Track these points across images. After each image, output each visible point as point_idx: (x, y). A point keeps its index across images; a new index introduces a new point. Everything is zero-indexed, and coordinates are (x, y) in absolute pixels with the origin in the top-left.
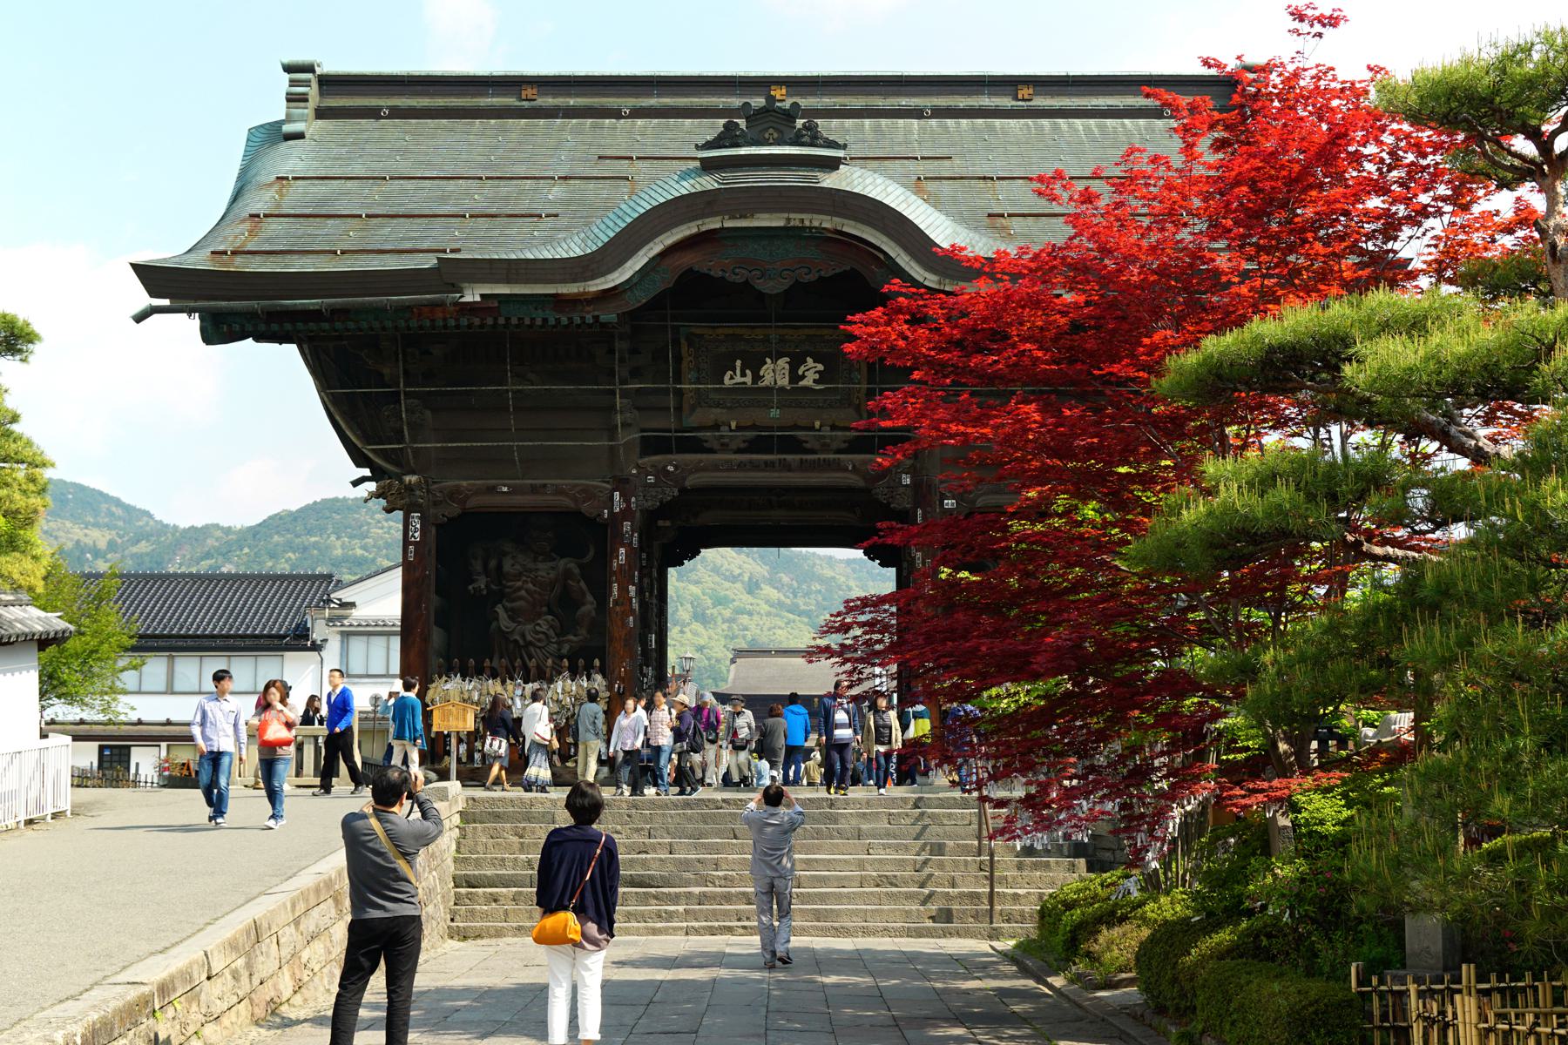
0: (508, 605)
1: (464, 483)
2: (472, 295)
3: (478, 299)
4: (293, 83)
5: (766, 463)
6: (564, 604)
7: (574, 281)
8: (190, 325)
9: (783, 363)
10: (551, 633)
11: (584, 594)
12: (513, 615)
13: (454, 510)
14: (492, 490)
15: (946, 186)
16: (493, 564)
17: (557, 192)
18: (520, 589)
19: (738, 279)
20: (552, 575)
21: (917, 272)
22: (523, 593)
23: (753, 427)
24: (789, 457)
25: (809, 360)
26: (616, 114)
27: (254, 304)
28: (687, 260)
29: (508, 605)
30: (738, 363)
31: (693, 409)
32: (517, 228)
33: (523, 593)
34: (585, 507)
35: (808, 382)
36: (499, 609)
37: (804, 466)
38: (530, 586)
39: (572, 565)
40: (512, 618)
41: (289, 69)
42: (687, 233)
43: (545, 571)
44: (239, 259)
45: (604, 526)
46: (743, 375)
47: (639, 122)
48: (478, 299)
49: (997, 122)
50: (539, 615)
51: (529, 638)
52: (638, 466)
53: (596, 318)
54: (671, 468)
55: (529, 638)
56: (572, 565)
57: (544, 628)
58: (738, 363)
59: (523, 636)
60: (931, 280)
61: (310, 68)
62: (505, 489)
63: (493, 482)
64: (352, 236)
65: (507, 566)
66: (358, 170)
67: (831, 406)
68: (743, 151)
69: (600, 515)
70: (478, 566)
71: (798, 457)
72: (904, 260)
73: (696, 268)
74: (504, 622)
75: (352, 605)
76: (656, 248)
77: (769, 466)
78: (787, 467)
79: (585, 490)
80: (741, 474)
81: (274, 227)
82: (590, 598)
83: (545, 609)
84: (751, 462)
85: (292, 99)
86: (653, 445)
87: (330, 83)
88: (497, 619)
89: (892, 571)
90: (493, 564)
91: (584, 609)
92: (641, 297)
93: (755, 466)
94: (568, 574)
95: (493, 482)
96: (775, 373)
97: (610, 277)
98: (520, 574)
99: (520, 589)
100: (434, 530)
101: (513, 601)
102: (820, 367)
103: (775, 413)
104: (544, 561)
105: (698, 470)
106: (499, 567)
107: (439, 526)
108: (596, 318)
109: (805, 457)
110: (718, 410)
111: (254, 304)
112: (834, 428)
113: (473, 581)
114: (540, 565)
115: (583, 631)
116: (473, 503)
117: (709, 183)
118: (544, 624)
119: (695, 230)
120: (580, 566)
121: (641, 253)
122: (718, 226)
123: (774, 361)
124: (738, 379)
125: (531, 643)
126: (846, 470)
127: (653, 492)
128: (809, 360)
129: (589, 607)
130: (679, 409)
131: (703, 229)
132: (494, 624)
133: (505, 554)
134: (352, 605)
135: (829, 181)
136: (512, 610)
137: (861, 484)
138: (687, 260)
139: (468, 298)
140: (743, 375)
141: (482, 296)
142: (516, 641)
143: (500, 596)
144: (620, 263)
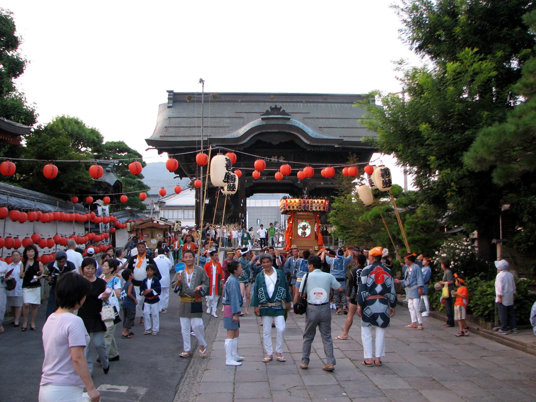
4: (169, 95)
7: (235, 142)
8: (156, 151)
15: (309, 120)
17: (228, 120)
21: (305, 141)
26: (238, 102)
32: (222, 130)
41: (167, 91)
44: (166, 138)
47: (243, 103)
49: (319, 104)
60: (308, 143)
61: (172, 92)
64: (187, 132)
66: (185, 115)
68: (270, 116)
75: (165, 202)
76: (252, 136)
81: (171, 130)
82: (233, 206)
85: (169, 99)
87: (176, 94)
93: (269, 179)
117: (264, 123)
135: (288, 123)
144: (245, 139)
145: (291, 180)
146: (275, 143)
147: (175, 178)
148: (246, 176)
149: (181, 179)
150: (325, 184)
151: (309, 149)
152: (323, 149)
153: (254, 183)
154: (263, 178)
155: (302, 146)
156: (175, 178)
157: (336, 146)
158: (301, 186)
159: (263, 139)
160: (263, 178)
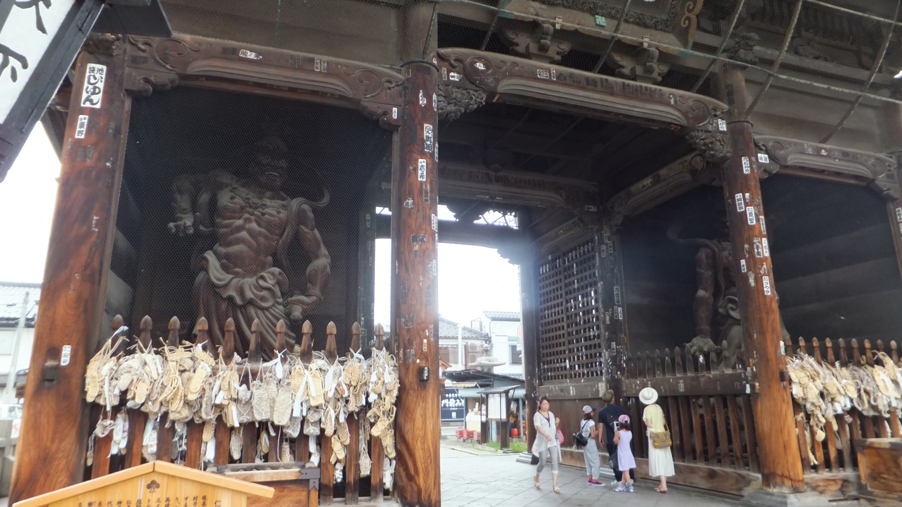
0: (222, 250)
1: (188, 37)
5: (587, 79)
6: (293, 258)
10: (277, 290)
11: (318, 247)
12: (229, 263)
14: (231, 54)
18: (240, 229)
20: (283, 215)
22: (244, 234)
29: (222, 250)
34: (370, 103)
36: (210, 256)
37: (626, 92)
38: (254, 225)
40: (226, 268)
43: (274, 209)
45: (391, 128)
50: (263, 267)
51: (249, 295)
52: (440, 57)
54: (480, 66)
55: (249, 295)
57: (270, 282)
59: (241, 292)
62: (251, 56)
63: (234, 43)
65: (225, 199)
67: (655, 28)
69: (387, 113)
70: (184, 202)
71: (620, 80)
74: (215, 271)
77: (590, 85)
82: (324, 250)
83: (270, 259)
84: (571, 75)
88: (205, 269)
93: (575, 83)
94: (300, 218)
95: (234, 43)
98: (242, 208)
99: (240, 229)
100: (128, 104)
101: (229, 244)
103: (601, 20)
104: (271, 198)
105: (512, 75)
106: (213, 202)
107: (137, 97)
109: (627, 82)
114: (268, 202)
115: (316, 291)
116: (198, 66)
118: (271, 276)
120: (315, 210)
125: (251, 302)
126: (668, 104)
127: (457, 93)
129: (322, 261)
132: (201, 276)
133: (221, 186)
136: (227, 256)
137: (684, 122)
142: (230, 299)
148: (443, 42)
158: (724, 150)
160: (543, 75)
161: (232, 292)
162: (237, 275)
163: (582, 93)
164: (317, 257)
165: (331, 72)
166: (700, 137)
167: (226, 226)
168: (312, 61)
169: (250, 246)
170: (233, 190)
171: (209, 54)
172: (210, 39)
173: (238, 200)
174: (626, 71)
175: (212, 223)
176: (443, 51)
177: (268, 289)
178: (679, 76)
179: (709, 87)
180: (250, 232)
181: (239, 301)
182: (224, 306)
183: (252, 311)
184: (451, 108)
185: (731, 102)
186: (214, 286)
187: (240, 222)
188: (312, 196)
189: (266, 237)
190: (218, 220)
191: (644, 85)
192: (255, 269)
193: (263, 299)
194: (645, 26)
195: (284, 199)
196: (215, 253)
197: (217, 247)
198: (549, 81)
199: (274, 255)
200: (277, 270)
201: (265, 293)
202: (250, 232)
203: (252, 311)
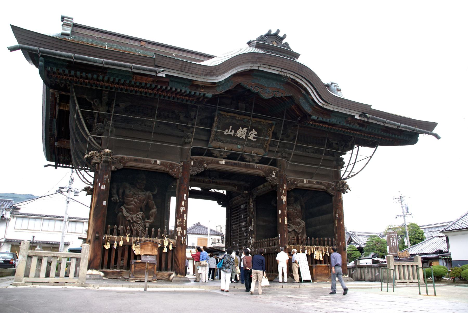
0: (127, 207)
1: (126, 156)
2: (163, 75)
3: (164, 76)
5: (234, 163)
6: (146, 209)
7: (206, 75)
9: (245, 129)
11: (154, 206)
12: (129, 210)
13: (121, 166)
16: (121, 191)
18: (132, 201)
19: (255, 91)
22: (133, 202)
23: (232, 150)
24: (242, 163)
25: (253, 130)
27: (72, 55)
28: (240, 80)
29: (127, 207)
30: (231, 127)
31: (212, 141)
33: (133, 202)
35: (251, 138)
36: (122, 207)
37: (246, 166)
38: (136, 200)
39: (150, 194)
40: (127, 211)
42: (246, 68)
43: (142, 195)
46: (231, 131)
48: (164, 76)
50: (138, 212)
51: (134, 220)
53: (204, 94)
55: (134, 220)
56: (150, 194)
57: (140, 216)
58: (231, 127)
59: (132, 219)
60: (320, 103)
65: (127, 192)
67: (257, 147)
71: (244, 163)
72: (314, 95)
73: (242, 84)
74: (125, 213)
75: (19, 209)
77: (235, 165)
78: (240, 166)
79: (171, 165)
80: (226, 166)
82: (155, 207)
84: (229, 162)
86: (195, 152)
88: (122, 212)
89: (225, 209)
90: (121, 191)
91: (154, 210)
92: (221, 90)
93: (231, 164)
94: (149, 198)
96: (241, 133)
97: (218, 78)
101: (128, 205)
102: (256, 133)
103: (239, 147)
105: (211, 163)
106: (124, 192)
108: (204, 94)
109: (247, 163)
110: (220, 143)
111: (72, 55)
112: (256, 154)
113: (114, 197)
114: (140, 193)
115: (152, 218)
118: (140, 214)
119: (249, 68)
121: (230, 71)
122: (257, 68)
123: (242, 129)
124: (229, 133)
125: (135, 222)
128: (253, 130)
130: (208, 141)
131: (253, 68)
132: (120, 213)
134: (19, 209)
136: (128, 208)
137: (264, 174)
138: (240, 80)
139: (160, 75)
140: (231, 131)
141: (166, 75)
142: (129, 221)
143: (123, 203)
145: (262, 170)
146: (266, 96)
147: (45, 166)
149: (56, 168)
150: (309, 182)
151: (314, 117)
152: (334, 120)
153: (205, 168)
154: (221, 162)
155: (307, 108)
156: (45, 166)
157: (357, 117)
158: (276, 182)
159: (248, 84)
160: (221, 162)
161: (130, 219)
162: (131, 214)
163: (232, 167)
164: (153, 209)
165: (162, 164)
166: (269, 178)
167: (128, 200)
168: (156, 161)
169: (135, 206)
170: (130, 189)
171: (131, 160)
172: (131, 157)
173: (131, 192)
174: (247, 159)
175: (123, 198)
176: (192, 157)
177: (140, 218)
178: (263, 161)
179: (274, 163)
180: (135, 202)
181: (132, 221)
182: (127, 222)
183: (135, 224)
184: (194, 173)
185: (280, 168)
186: (124, 216)
187: (132, 199)
188: (152, 191)
189: (139, 203)
190: (126, 198)
191: (252, 164)
192: (135, 212)
193: (138, 221)
194: (253, 147)
195: (143, 192)
196: (124, 207)
197: (125, 205)
198: (223, 164)
199: (141, 208)
200: (142, 213)
201: (138, 219)
202: (135, 202)
203: (135, 224)
